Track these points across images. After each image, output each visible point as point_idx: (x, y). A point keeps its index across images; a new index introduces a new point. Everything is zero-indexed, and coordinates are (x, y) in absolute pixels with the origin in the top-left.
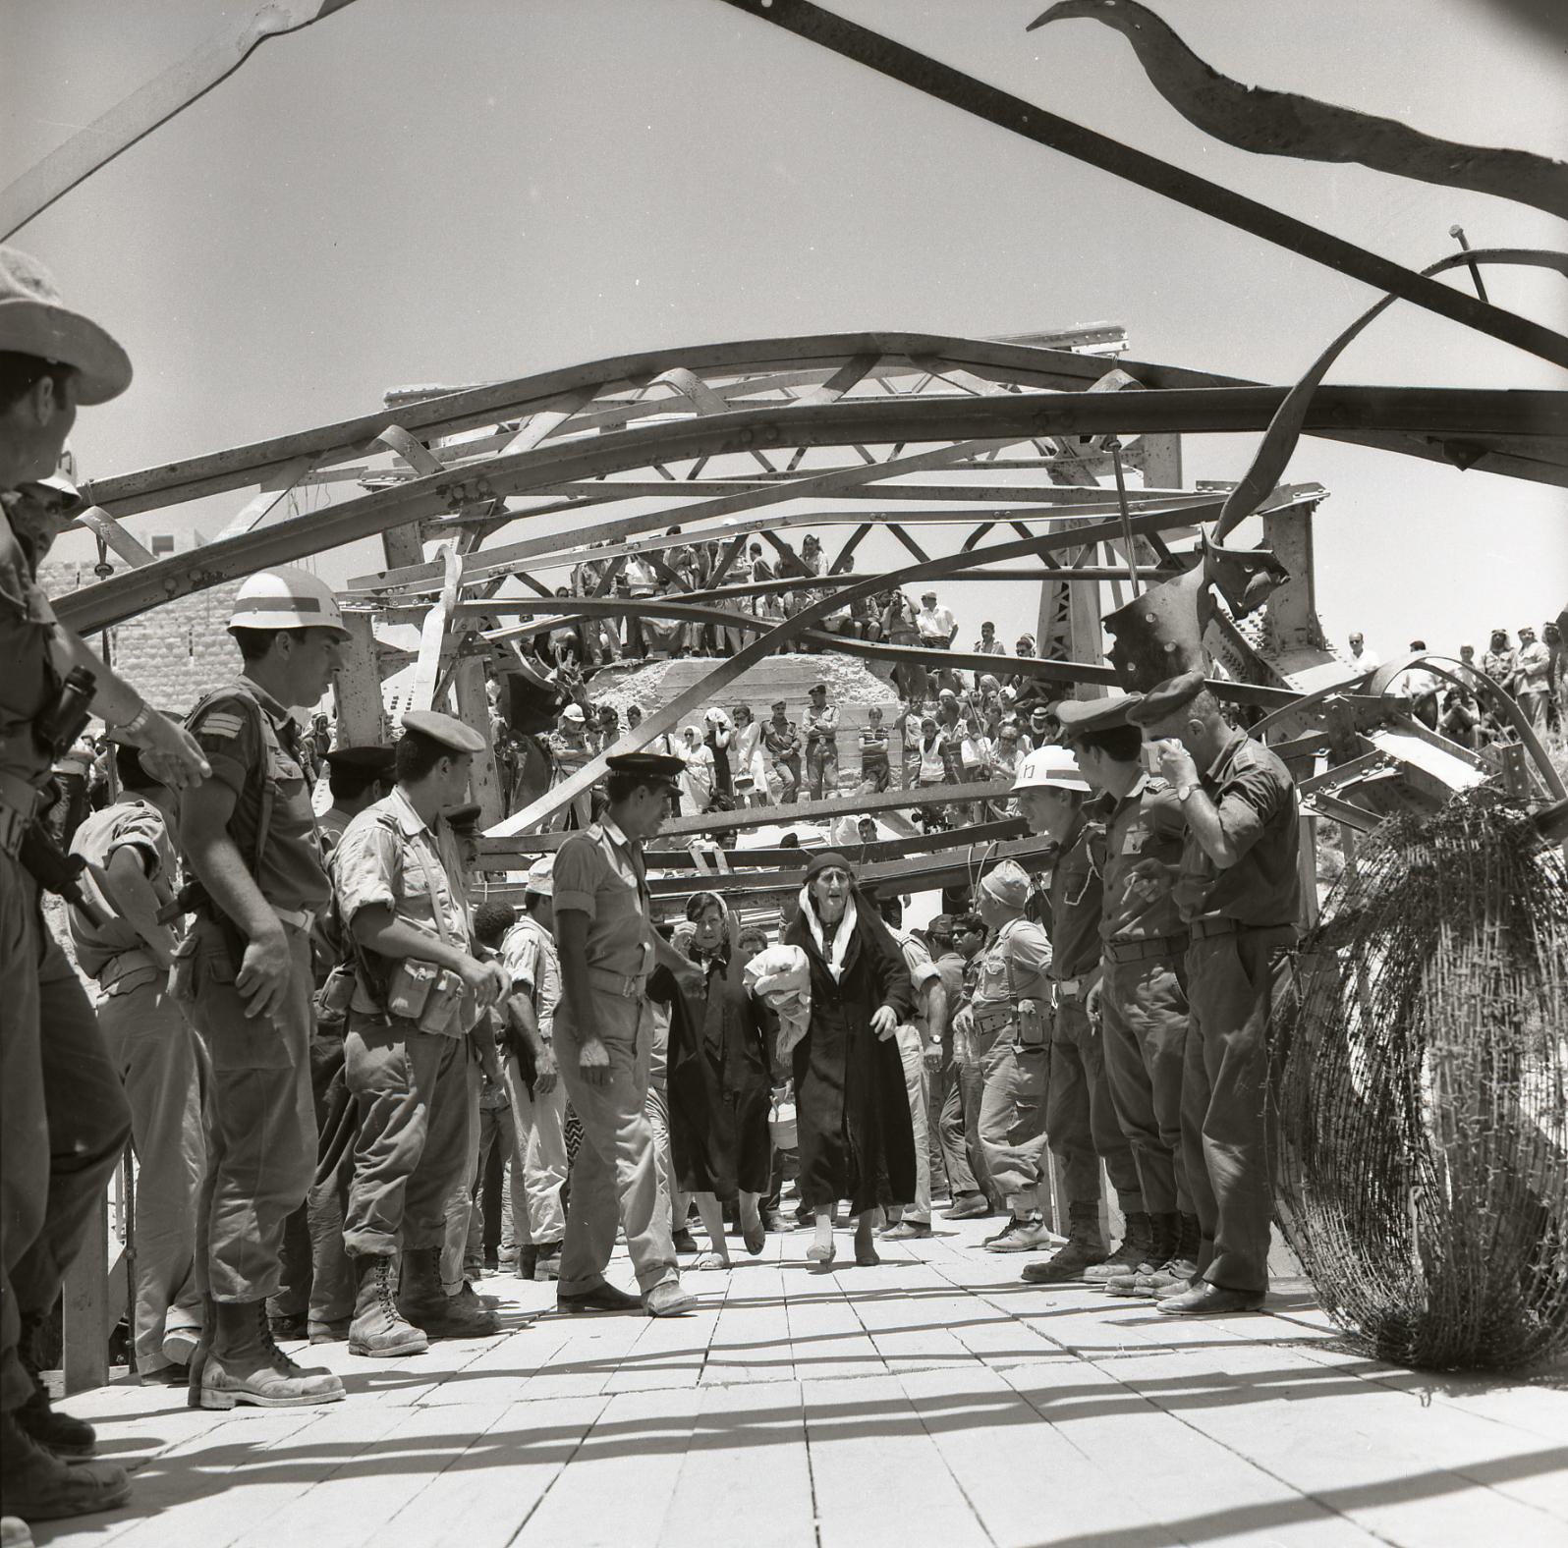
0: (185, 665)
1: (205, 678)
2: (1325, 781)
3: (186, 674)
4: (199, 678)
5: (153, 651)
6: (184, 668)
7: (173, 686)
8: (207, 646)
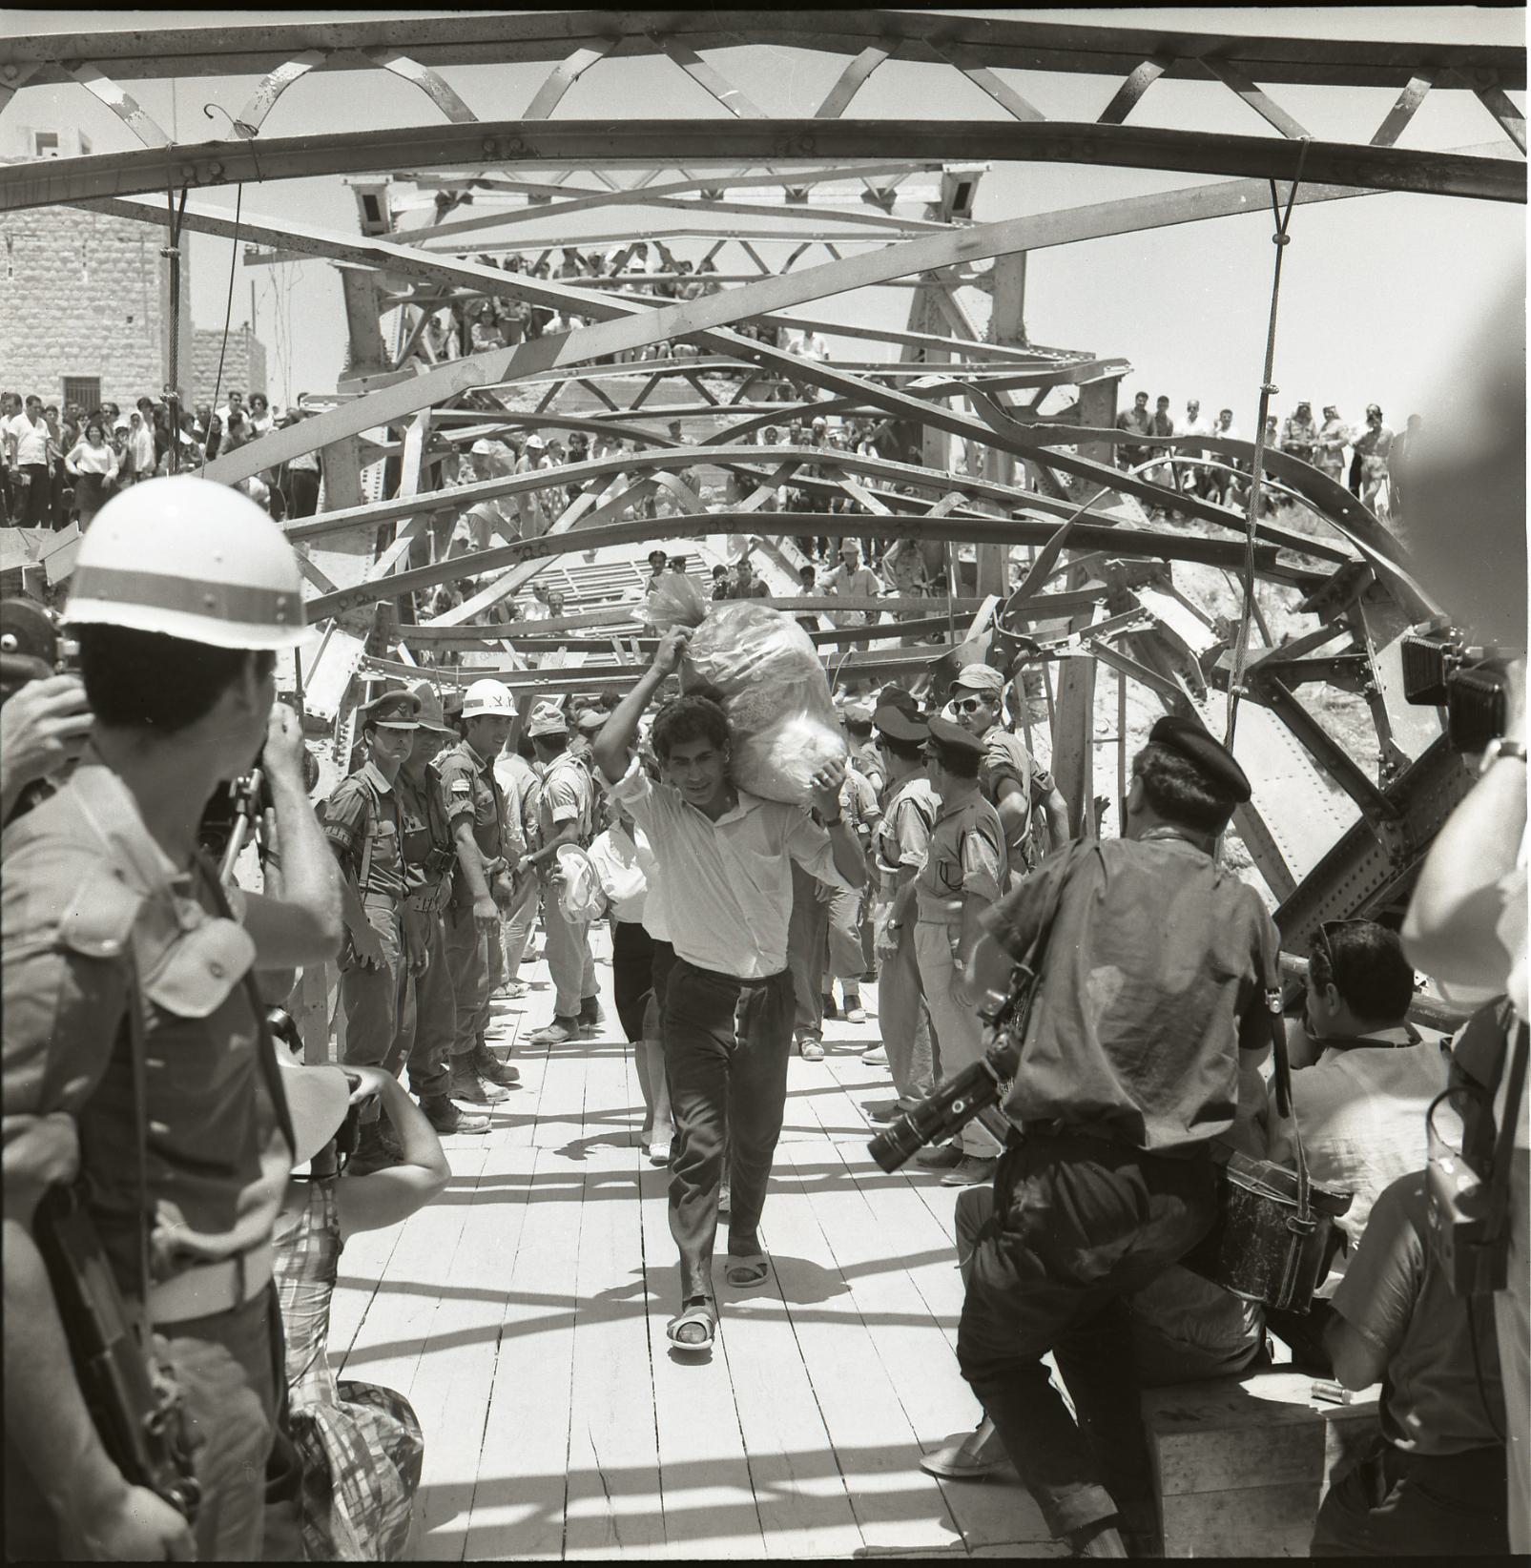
1: (99, 294)
3: (80, 289)
4: (92, 294)
5: (48, 264)
6: (78, 283)
7: (68, 300)
8: (101, 262)
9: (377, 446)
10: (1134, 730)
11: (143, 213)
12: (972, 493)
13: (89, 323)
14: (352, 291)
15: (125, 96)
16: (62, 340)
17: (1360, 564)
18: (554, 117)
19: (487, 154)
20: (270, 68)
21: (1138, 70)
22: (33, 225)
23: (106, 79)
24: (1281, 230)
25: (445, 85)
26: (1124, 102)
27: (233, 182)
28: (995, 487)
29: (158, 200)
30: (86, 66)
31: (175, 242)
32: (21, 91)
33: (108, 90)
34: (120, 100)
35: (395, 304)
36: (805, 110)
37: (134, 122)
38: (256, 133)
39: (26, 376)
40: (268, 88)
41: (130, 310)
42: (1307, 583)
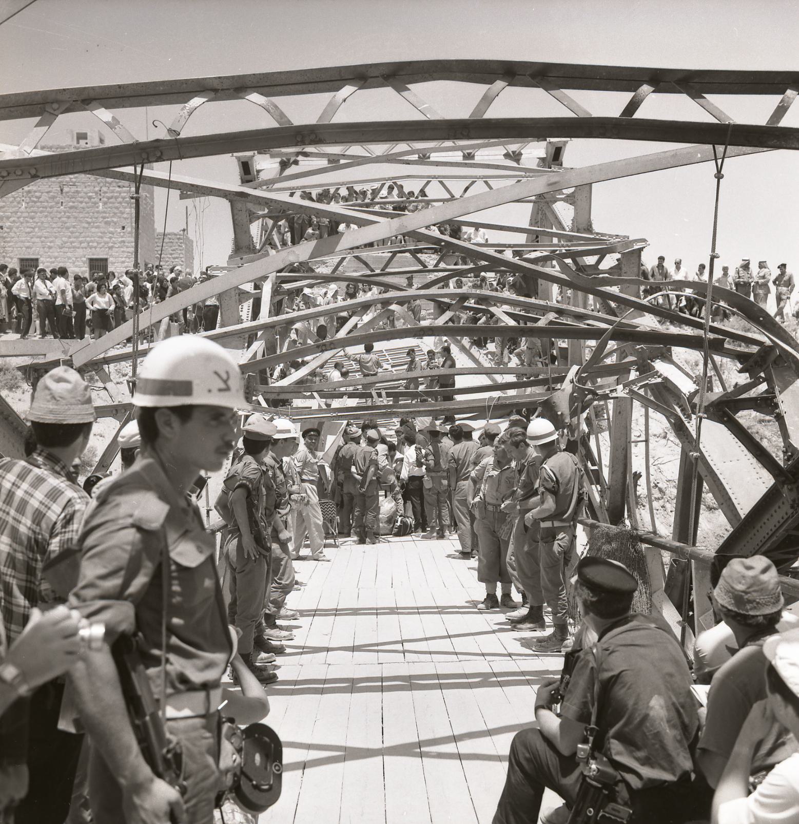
0: (98, 207)
2: (633, 382)
3: (98, 212)
4: (104, 215)
5: (82, 199)
8: (109, 198)
9: (248, 292)
10: (655, 435)
11: (123, 176)
12: (560, 312)
13: (102, 230)
14: (236, 212)
15: (113, 117)
16: (88, 239)
17: (770, 347)
18: (332, 122)
19: (298, 142)
20: (186, 101)
21: (640, 89)
22: (74, 180)
23: (103, 109)
24: (719, 171)
25: (276, 107)
26: (633, 106)
27: (168, 160)
28: (573, 309)
29: (129, 170)
30: (94, 103)
31: (137, 192)
32: (60, 116)
33: (104, 114)
34: (110, 119)
35: (258, 218)
36: (463, 113)
37: (117, 130)
38: (179, 134)
39: (69, 258)
40: (185, 111)
41: (124, 223)
42: (741, 357)
